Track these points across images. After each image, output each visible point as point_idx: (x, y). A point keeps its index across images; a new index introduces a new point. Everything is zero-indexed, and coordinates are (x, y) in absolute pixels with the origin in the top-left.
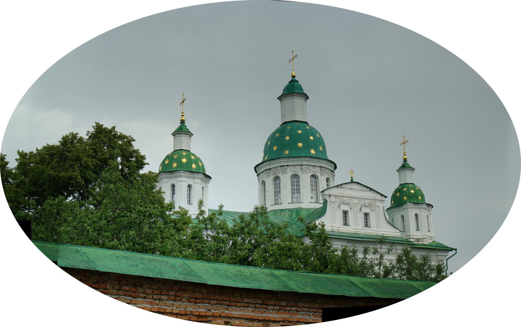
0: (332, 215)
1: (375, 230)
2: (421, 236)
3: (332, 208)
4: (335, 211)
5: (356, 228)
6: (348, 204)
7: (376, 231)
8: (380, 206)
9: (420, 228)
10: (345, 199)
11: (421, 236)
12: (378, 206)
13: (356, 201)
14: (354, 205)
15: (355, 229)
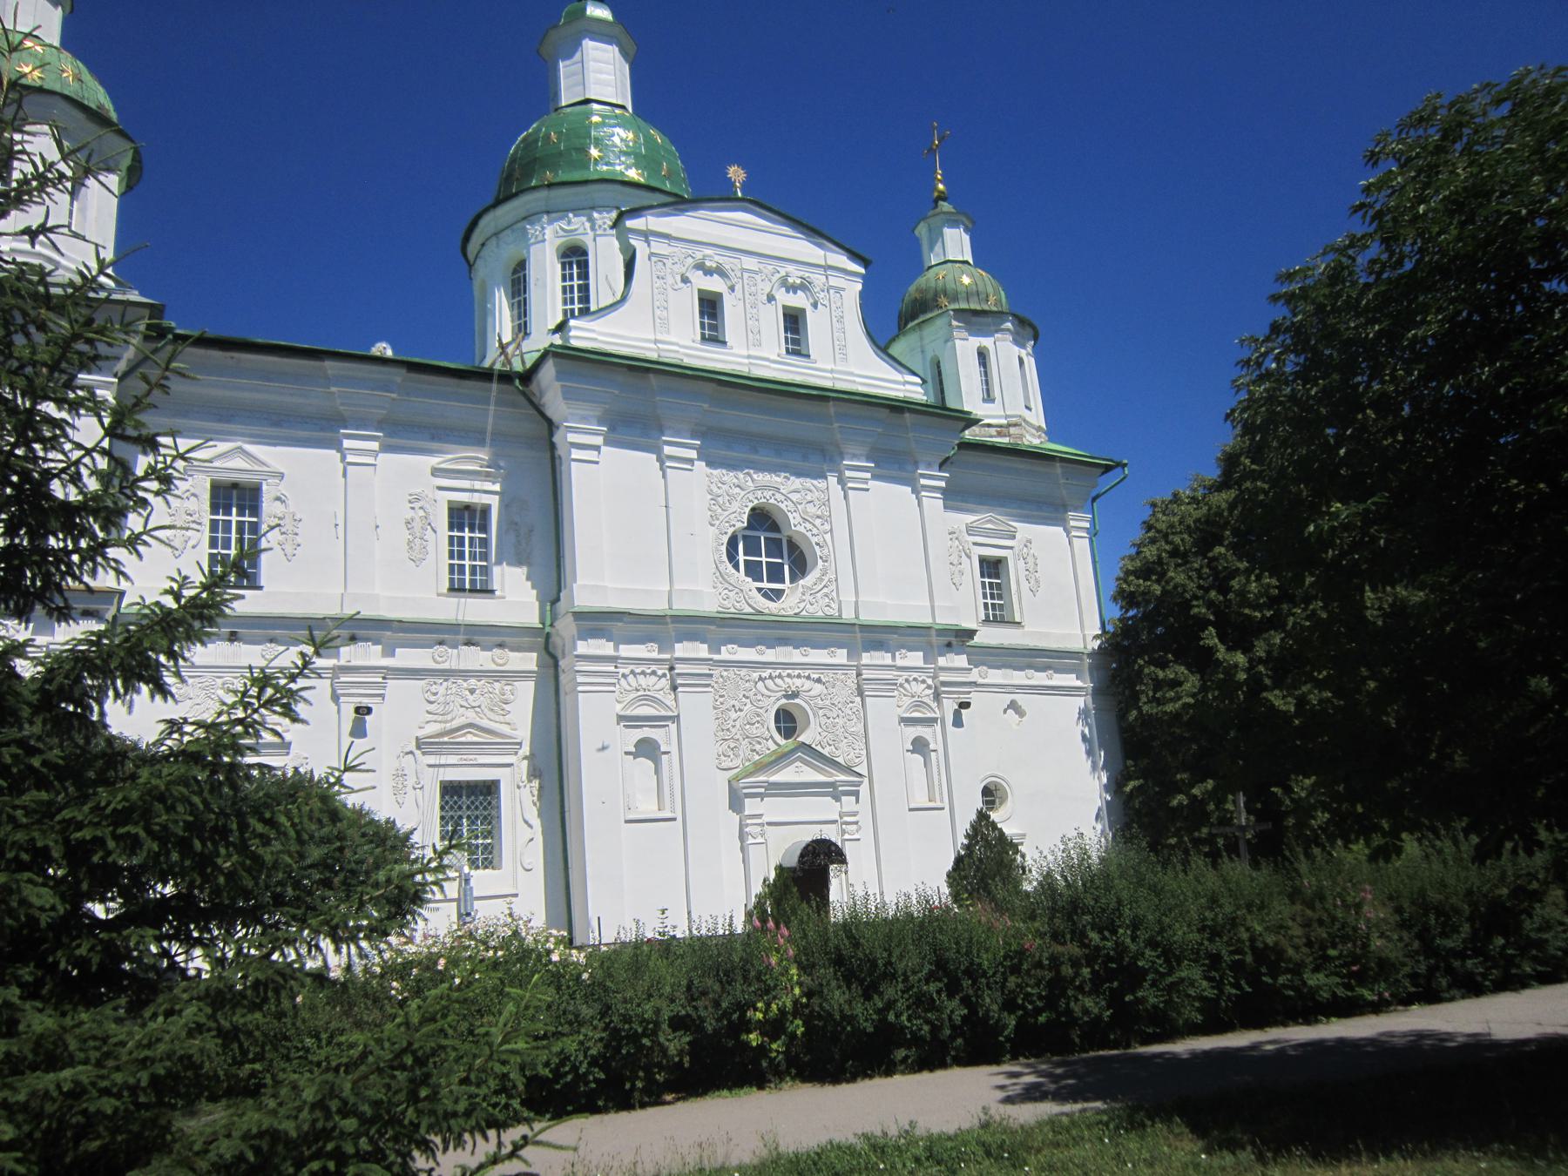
0: (657, 304)
1: (829, 367)
2: (1000, 417)
3: (655, 279)
4: (670, 289)
5: (752, 353)
6: (720, 272)
7: (832, 371)
8: (843, 289)
9: (997, 393)
10: (708, 252)
11: (1000, 417)
12: (839, 290)
13: (750, 263)
14: (746, 275)
15: (749, 357)
